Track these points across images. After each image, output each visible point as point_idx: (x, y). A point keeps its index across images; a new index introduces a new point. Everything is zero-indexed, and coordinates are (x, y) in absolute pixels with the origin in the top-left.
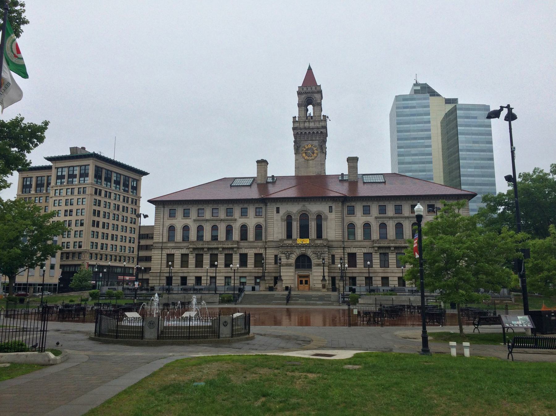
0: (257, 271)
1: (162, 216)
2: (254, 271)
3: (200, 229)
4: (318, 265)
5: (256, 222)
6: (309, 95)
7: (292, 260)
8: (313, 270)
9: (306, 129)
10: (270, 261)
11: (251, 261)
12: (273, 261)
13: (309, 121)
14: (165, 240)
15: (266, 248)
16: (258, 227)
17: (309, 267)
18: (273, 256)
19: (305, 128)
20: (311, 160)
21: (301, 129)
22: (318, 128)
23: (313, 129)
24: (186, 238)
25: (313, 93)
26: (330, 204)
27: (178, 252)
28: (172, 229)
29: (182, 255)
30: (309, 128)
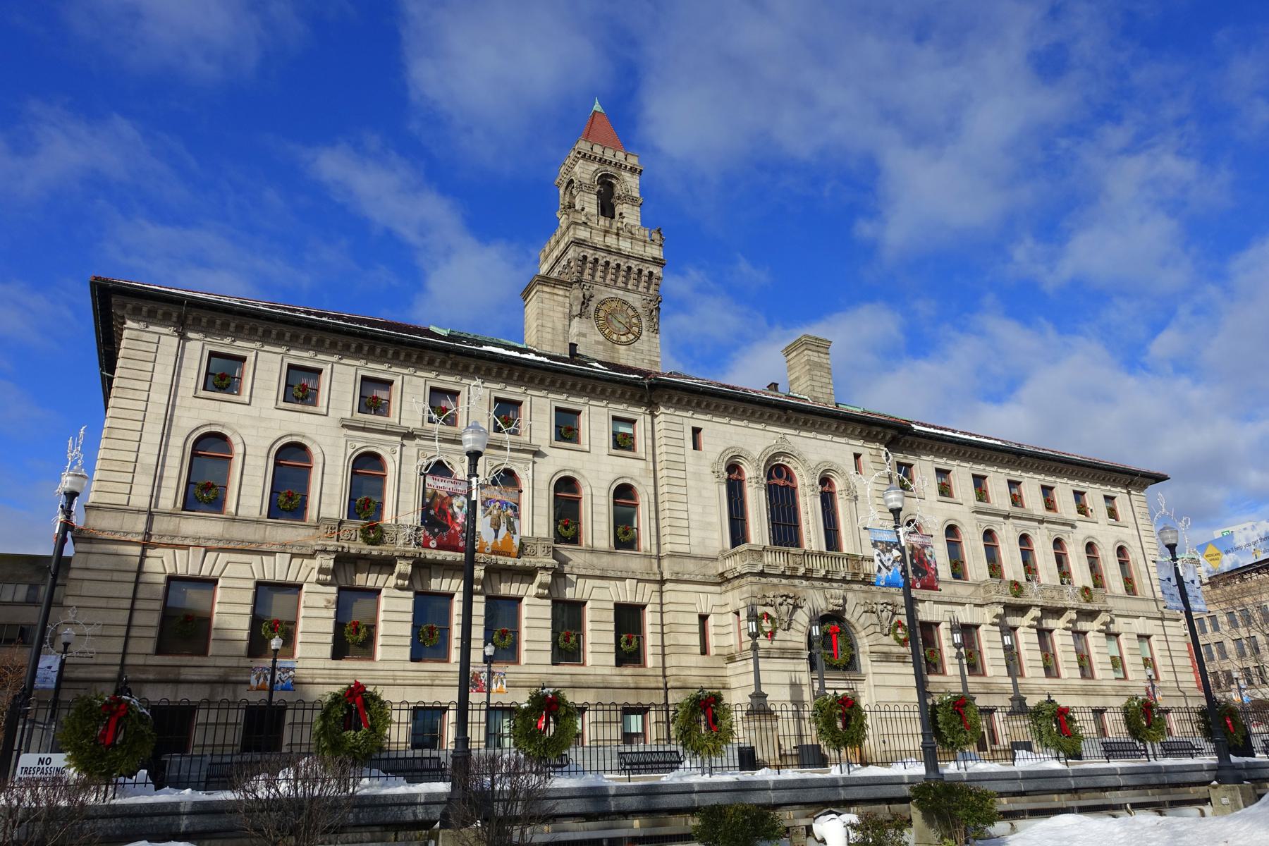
0: (631, 682)
1: (163, 375)
2: (617, 680)
3: (367, 468)
4: (886, 657)
5: (619, 471)
6: (611, 170)
7: (796, 637)
8: (870, 679)
9: (610, 252)
10: (683, 640)
11: (598, 636)
12: (696, 640)
13: (618, 234)
14: (170, 497)
15: (662, 582)
16: (624, 493)
17: (850, 665)
18: (696, 620)
19: (608, 251)
20: (622, 344)
21: (595, 248)
22: (643, 260)
23: (628, 257)
24: (288, 499)
25: (619, 166)
26: (857, 445)
27: (244, 571)
28: (211, 448)
29: (264, 588)
30: (619, 253)
